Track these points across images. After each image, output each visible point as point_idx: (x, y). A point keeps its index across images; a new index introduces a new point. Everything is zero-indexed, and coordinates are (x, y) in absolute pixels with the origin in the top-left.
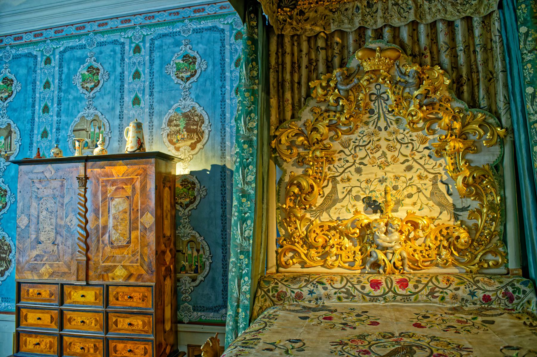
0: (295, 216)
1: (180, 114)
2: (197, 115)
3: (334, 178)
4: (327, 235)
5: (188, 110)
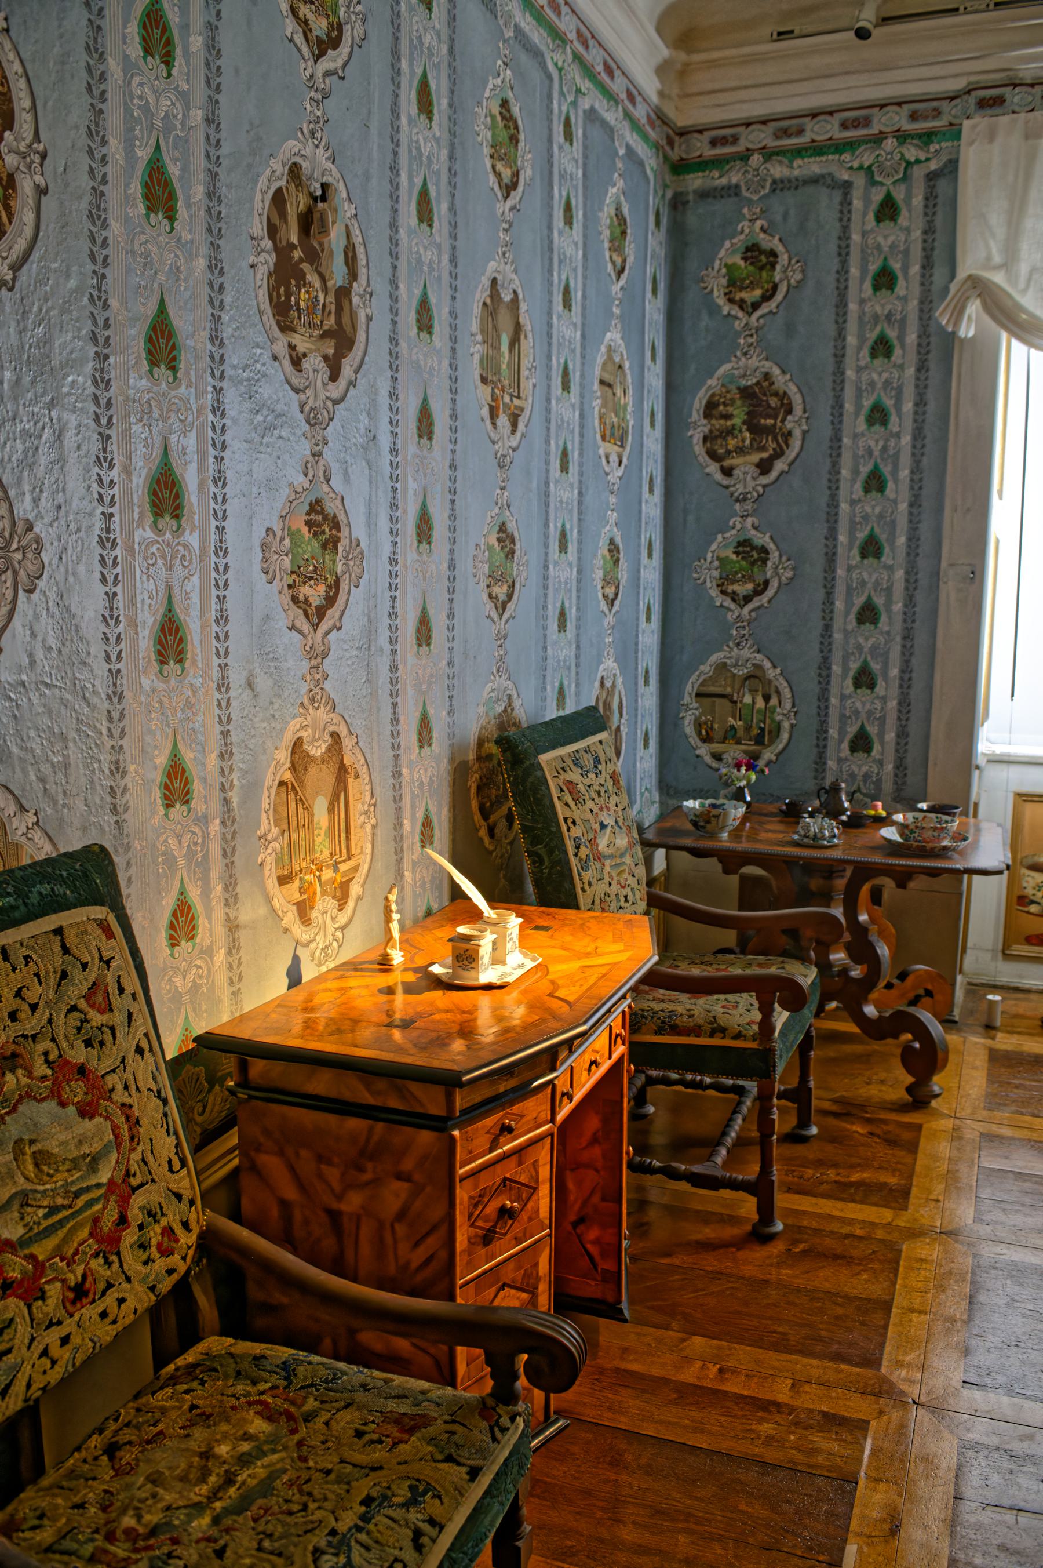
2: (776, 394)
5: (754, 381)
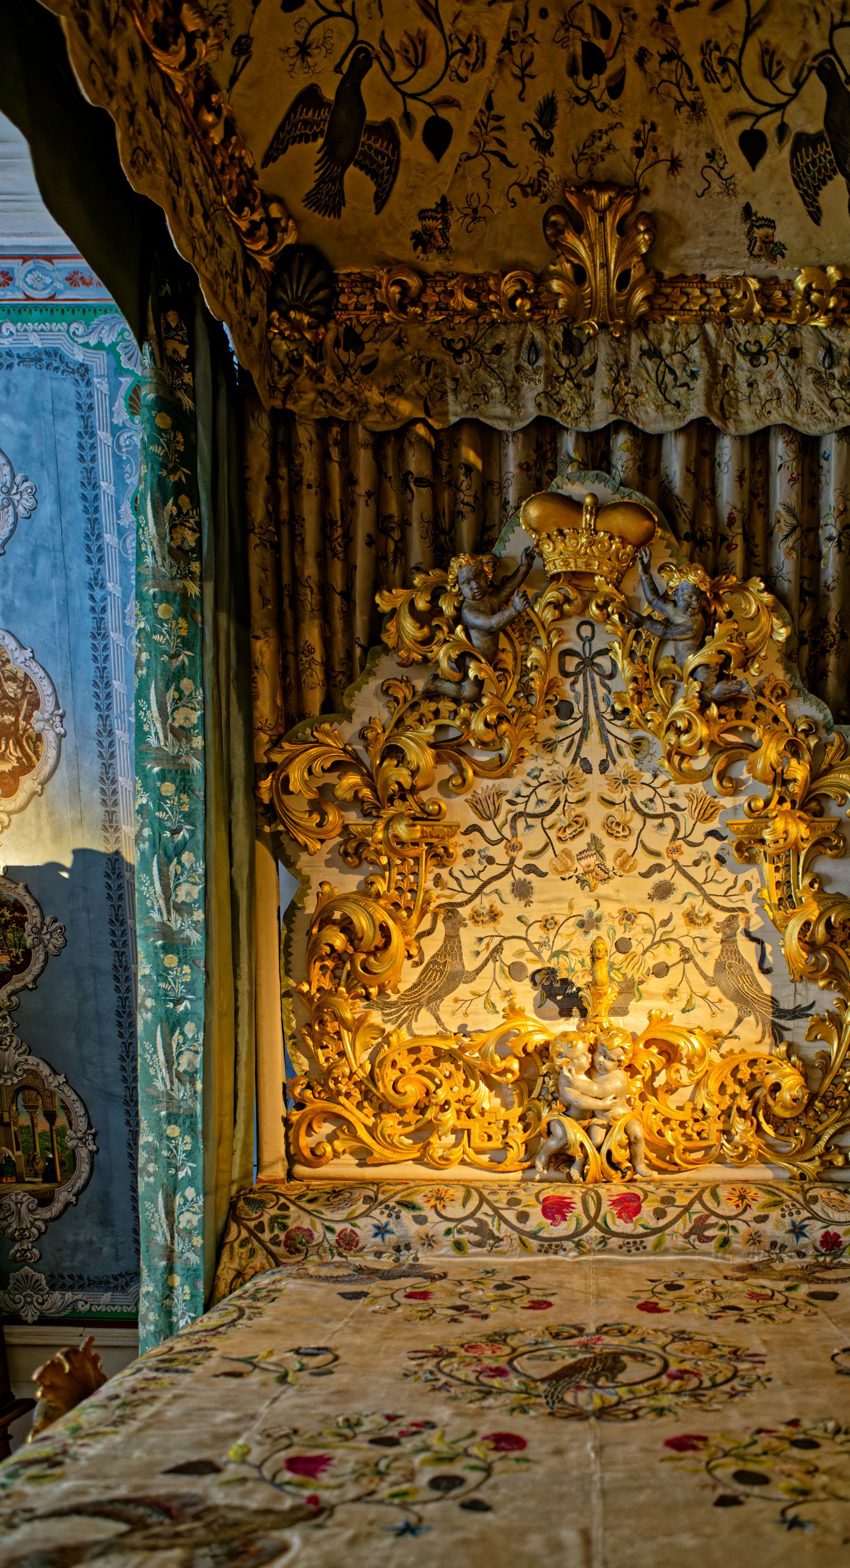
0: (337, 1017)
3: (451, 909)
4: (431, 1076)
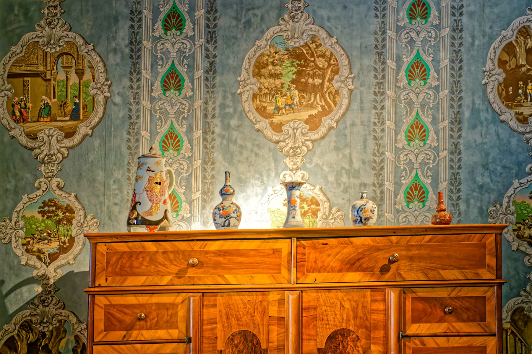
1: (283, 52)
5: (302, 43)
